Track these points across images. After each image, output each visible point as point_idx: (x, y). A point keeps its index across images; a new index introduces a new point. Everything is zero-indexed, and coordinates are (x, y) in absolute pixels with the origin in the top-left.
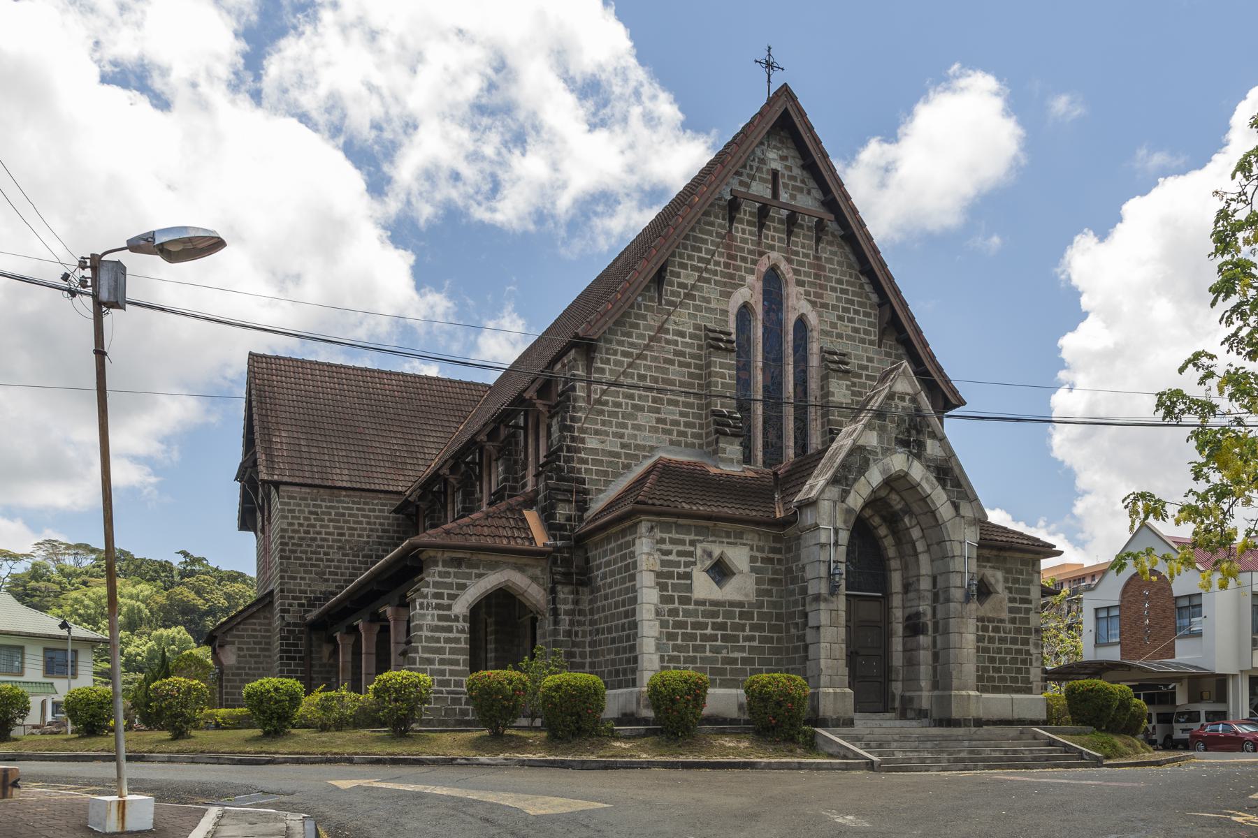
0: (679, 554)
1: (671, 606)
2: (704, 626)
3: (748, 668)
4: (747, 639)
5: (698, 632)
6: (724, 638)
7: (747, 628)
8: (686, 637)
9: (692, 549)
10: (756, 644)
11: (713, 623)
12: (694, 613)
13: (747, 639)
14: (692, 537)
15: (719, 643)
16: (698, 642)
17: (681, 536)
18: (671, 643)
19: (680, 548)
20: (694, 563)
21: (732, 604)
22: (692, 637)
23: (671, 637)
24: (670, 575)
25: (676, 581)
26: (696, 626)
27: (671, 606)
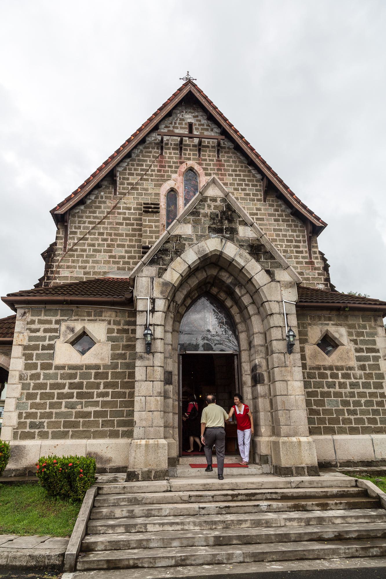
0: (45, 331)
1: (34, 372)
2: (63, 386)
3: (100, 420)
4: (100, 395)
5: (56, 392)
6: (80, 395)
7: (102, 386)
8: (43, 396)
9: (57, 326)
10: (109, 399)
11: (71, 384)
12: (55, 376)
13: (100, 395)
14: (58, 318)
15: (75, 400)
16: (55, 400)
17: (49, 318)
18: (30, 402)
19: (47, 326)
20: (58, 337)
21: (88, 367)
22: (50, 396)
23: (30, 396)
24: (36, 348)
25: (40, 352)
26: (54, 386)
27: (34, 372)
